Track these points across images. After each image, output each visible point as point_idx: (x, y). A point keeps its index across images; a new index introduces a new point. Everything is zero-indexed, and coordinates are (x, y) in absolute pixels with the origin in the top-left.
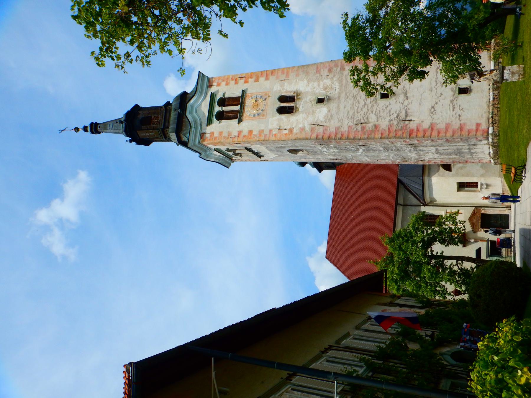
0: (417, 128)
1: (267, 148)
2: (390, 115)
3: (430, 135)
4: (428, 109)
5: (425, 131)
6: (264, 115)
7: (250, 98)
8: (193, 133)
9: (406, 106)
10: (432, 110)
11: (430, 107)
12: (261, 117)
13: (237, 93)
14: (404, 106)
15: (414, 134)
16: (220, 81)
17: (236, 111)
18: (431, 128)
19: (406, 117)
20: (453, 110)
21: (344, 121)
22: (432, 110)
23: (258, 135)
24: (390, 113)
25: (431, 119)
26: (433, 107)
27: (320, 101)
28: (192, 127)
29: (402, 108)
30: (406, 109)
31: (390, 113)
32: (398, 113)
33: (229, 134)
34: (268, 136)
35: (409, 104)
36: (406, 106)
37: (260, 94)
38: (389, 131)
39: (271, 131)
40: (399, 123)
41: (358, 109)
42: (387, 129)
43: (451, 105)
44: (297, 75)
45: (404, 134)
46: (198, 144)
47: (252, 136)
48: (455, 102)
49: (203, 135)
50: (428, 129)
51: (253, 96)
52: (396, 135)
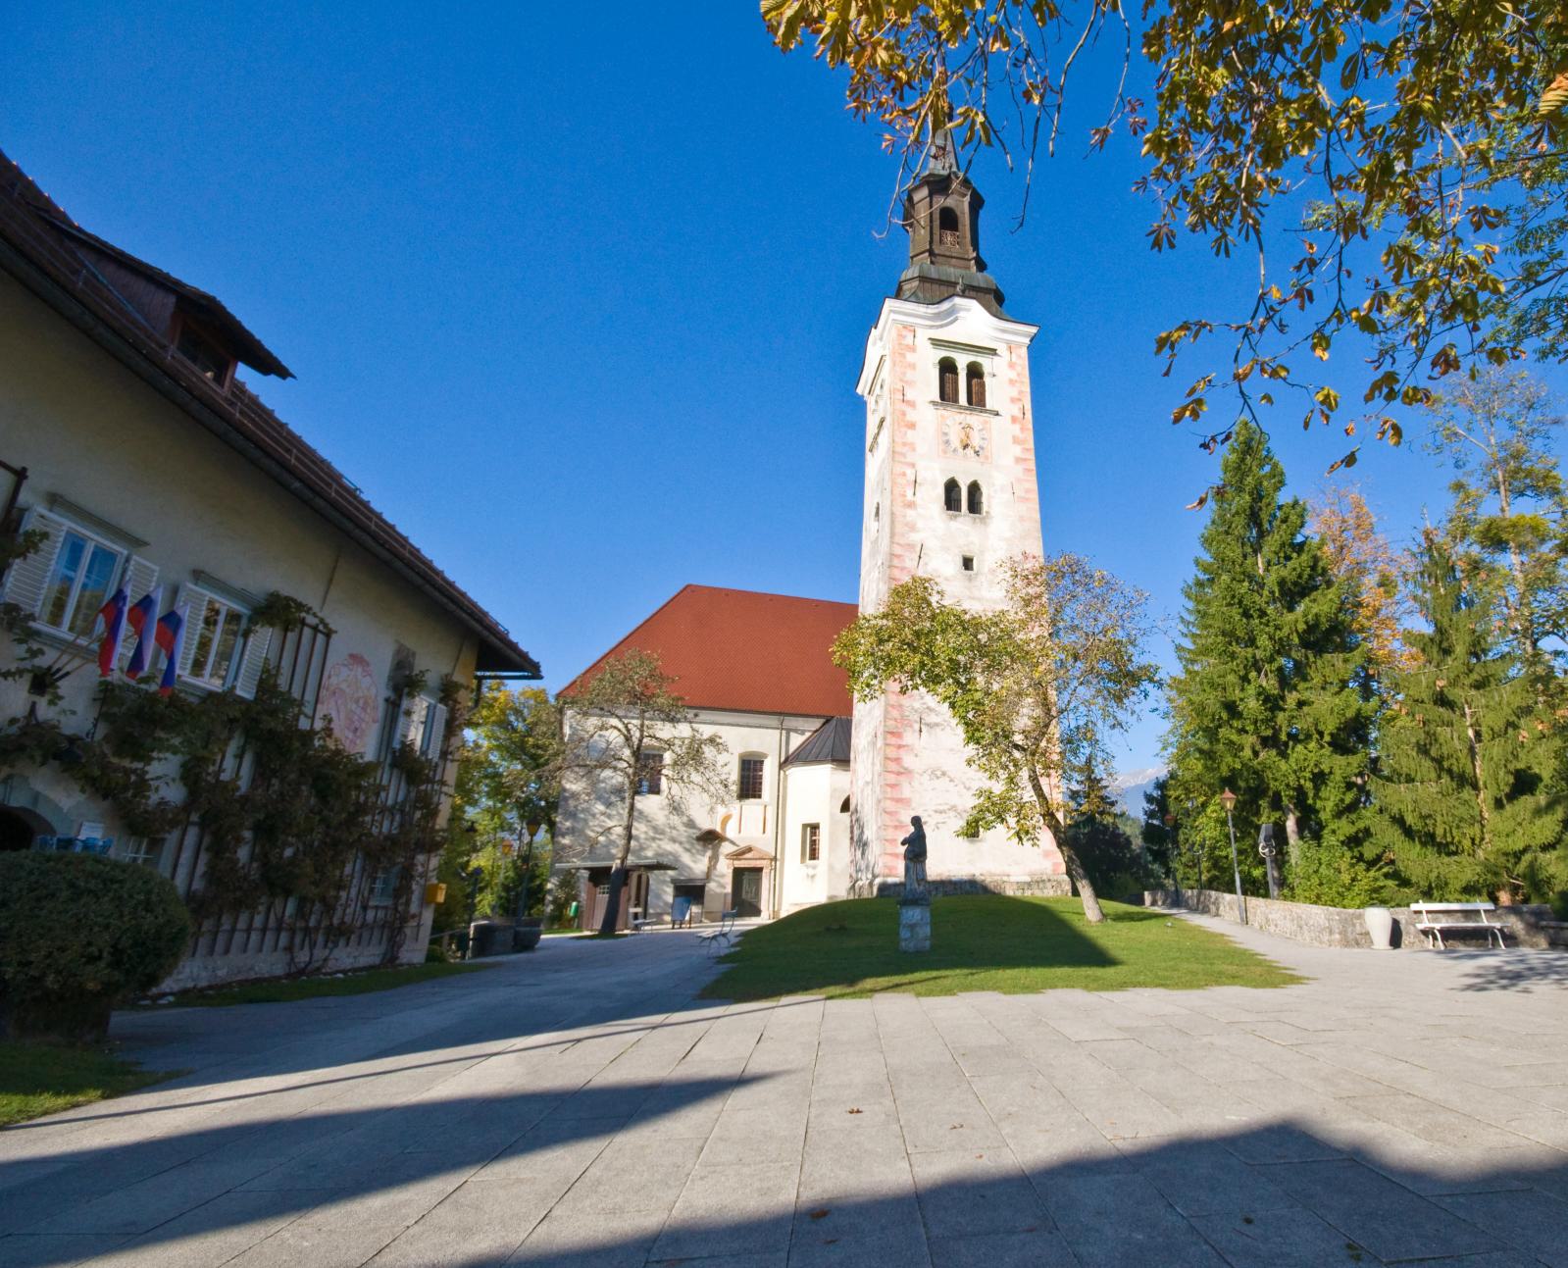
1: (884, 460)
5: (897, 760)
6: (945, 452)
10: (939, 773)
11: (943, 769)
13: (991, 402)
15: (893, 740)
16: (1019, 369)
17: (955, 400)
19: (928, 725)
20: (936, 811)
22: (939, 773)
26: (944, 774)
27: (968, 563)
33: (910, 383)
34: (903, 460)
39: (913, 465)
43: (946, 807)
44: (1022, 519)
47: (903, 429)
48: (952, 814)
50: (902, 767)
52: (893, 706)
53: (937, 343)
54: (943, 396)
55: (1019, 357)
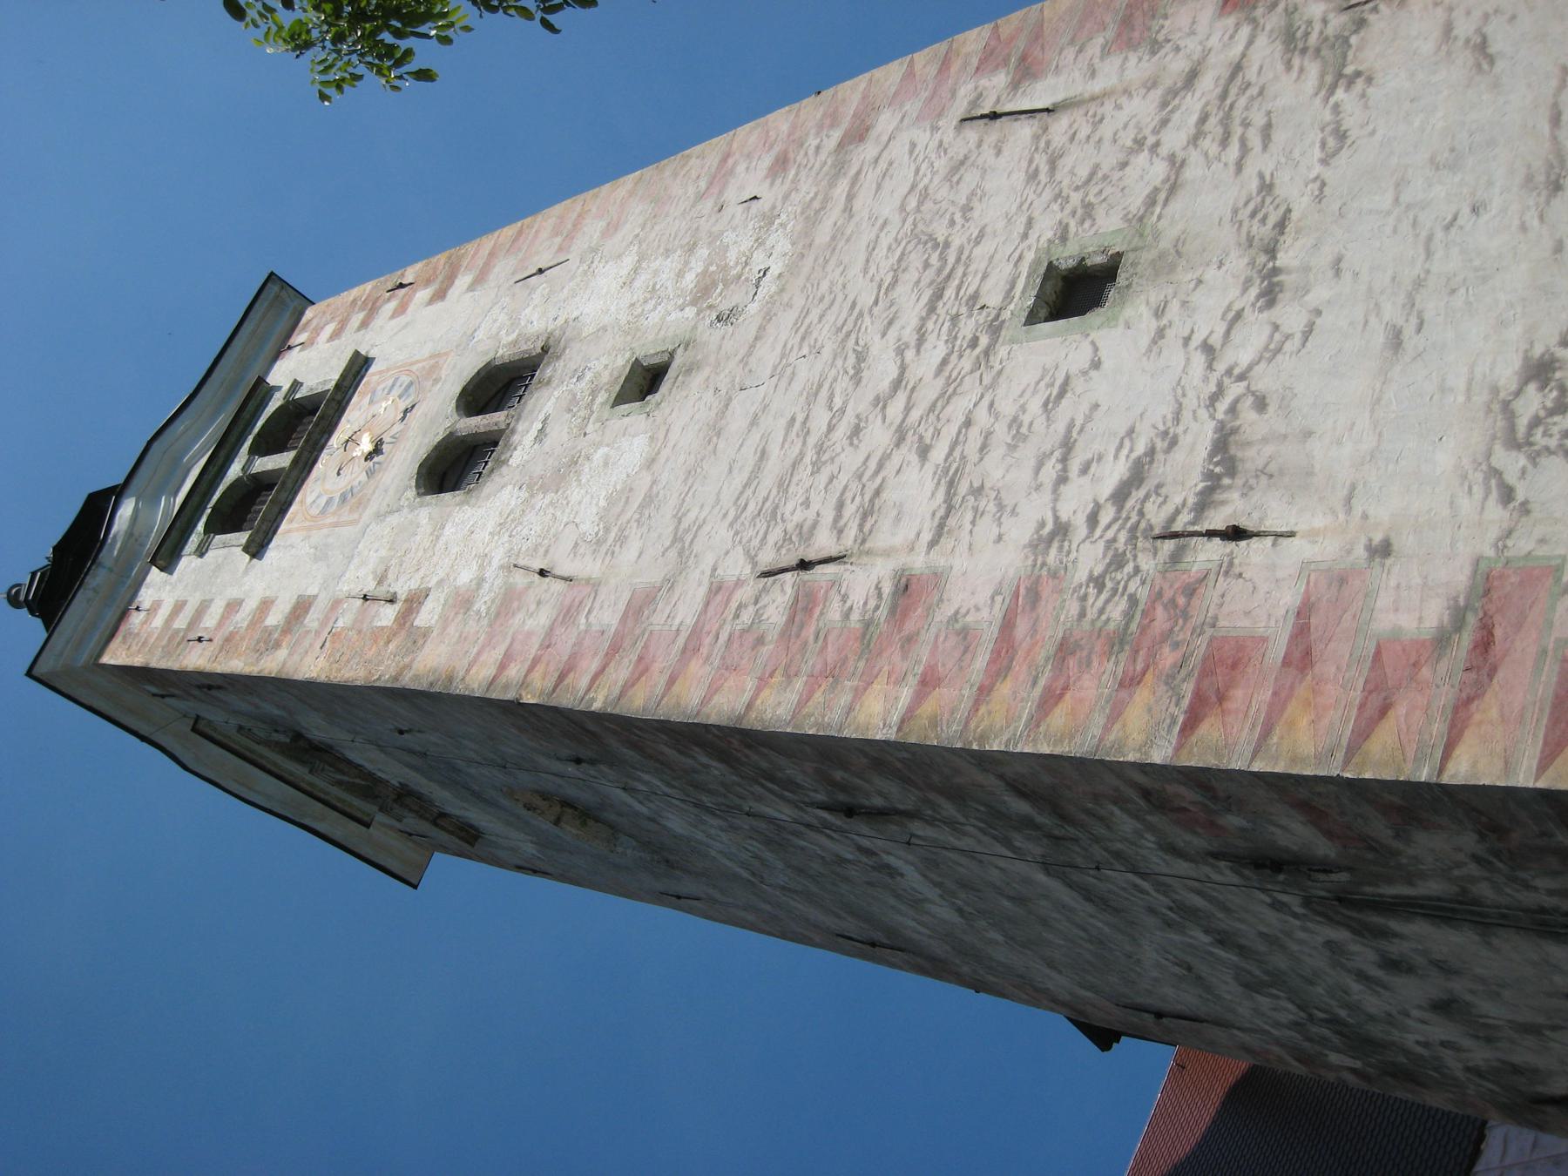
0: (1301, 630)
2: (1062, 479)
3: (1438, 728)
4: (1480, 398)
9: (1242, 377)
11: (1508, 372)
14: (1221, 367)
18: (1467, 639)
21: (697, 548)
24: (1064, 460)
25: (1496, 514)
28: (100, 564)
29: (1190, 402)
30: (1233, 410)
31: (1064, 460)
32: (1140, 449)
35: (1279, 350)
36: (1242, 377)
38: (996, 654)
40: (1118, 562)
41: (831, 428)
42: (987, 620)
45: (1142, 696)
50: (1441, 641)
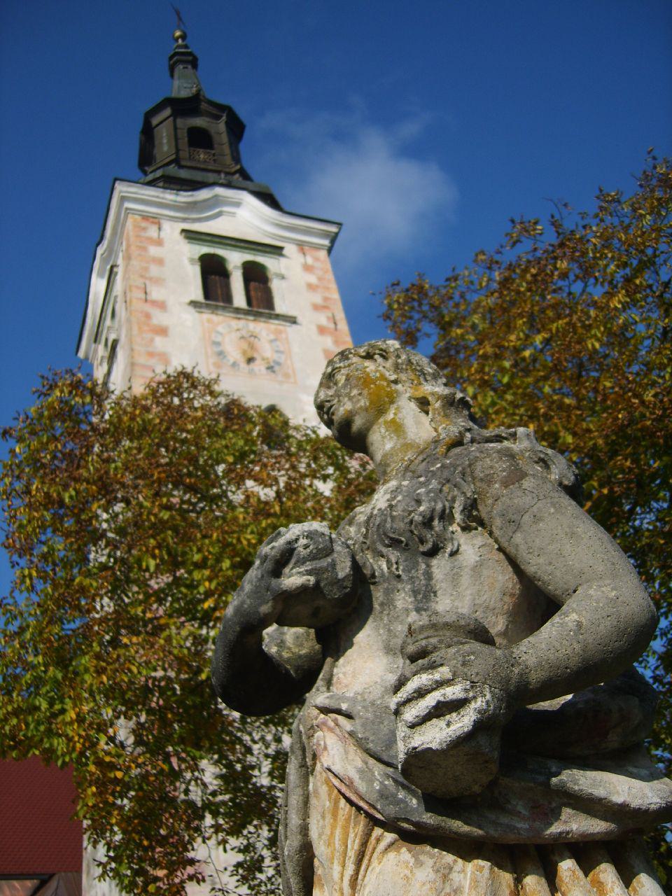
7: (272, 337)
8: (157, 197)
12: (211, 361)
17: (228, 298)
23: (151, 349)
37: (289, 362)
46: (127, 209)
47: (149, 336)
49: (153, 223)
51: (278, 343)
53: (191, 236)
54: (208, 294)
55: (317, 259)
